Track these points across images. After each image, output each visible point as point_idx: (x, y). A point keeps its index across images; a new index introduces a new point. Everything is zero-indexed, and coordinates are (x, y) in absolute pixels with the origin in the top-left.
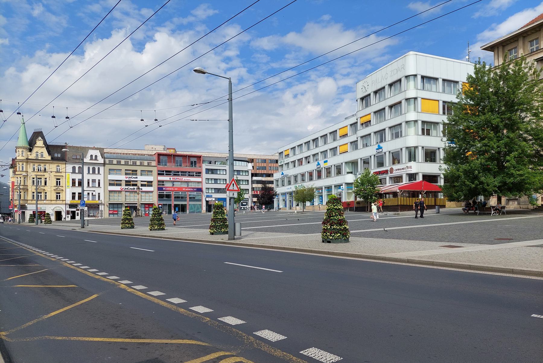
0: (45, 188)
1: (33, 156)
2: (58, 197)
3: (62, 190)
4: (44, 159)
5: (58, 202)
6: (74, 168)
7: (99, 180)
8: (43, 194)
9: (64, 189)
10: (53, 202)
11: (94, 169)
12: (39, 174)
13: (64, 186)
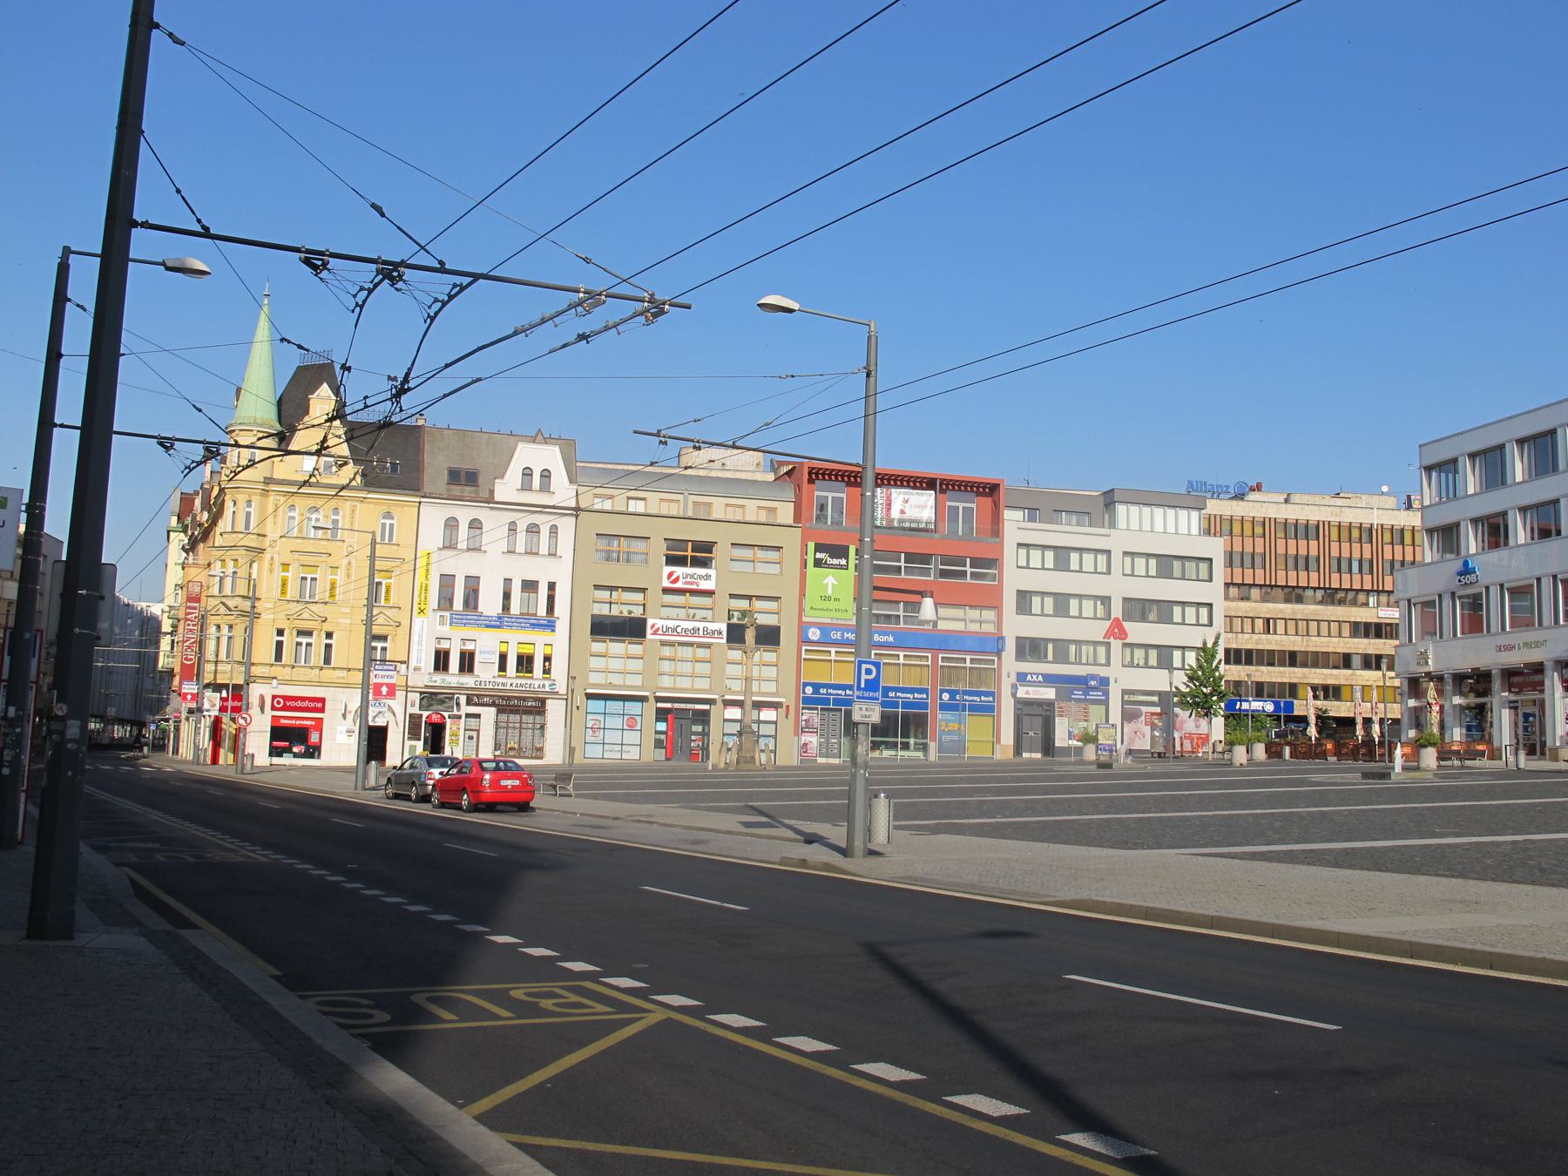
6: (451, 524)
7: (552, 586)
11: (533, 529)
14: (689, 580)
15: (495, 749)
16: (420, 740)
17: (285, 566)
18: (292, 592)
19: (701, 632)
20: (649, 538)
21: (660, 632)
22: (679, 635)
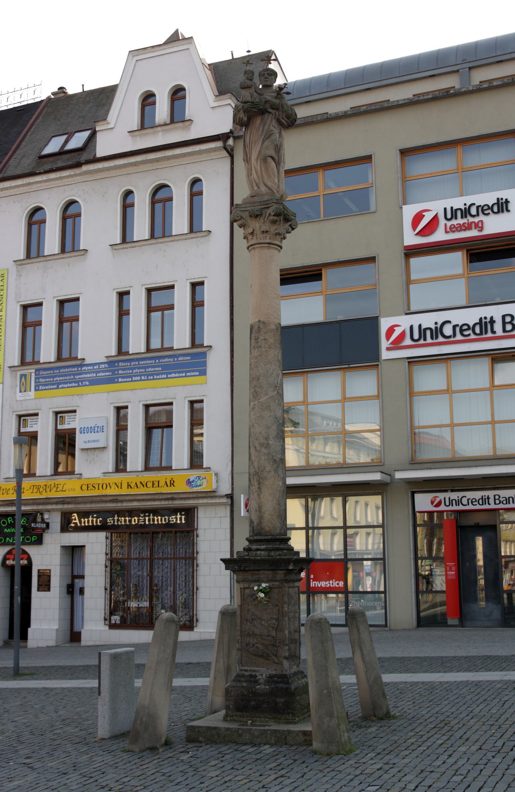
14: (460, 221)
15: (111, 614)
19: (498, 327)
20: (368, 159)
21: (408, 341)
22: (449, 340)
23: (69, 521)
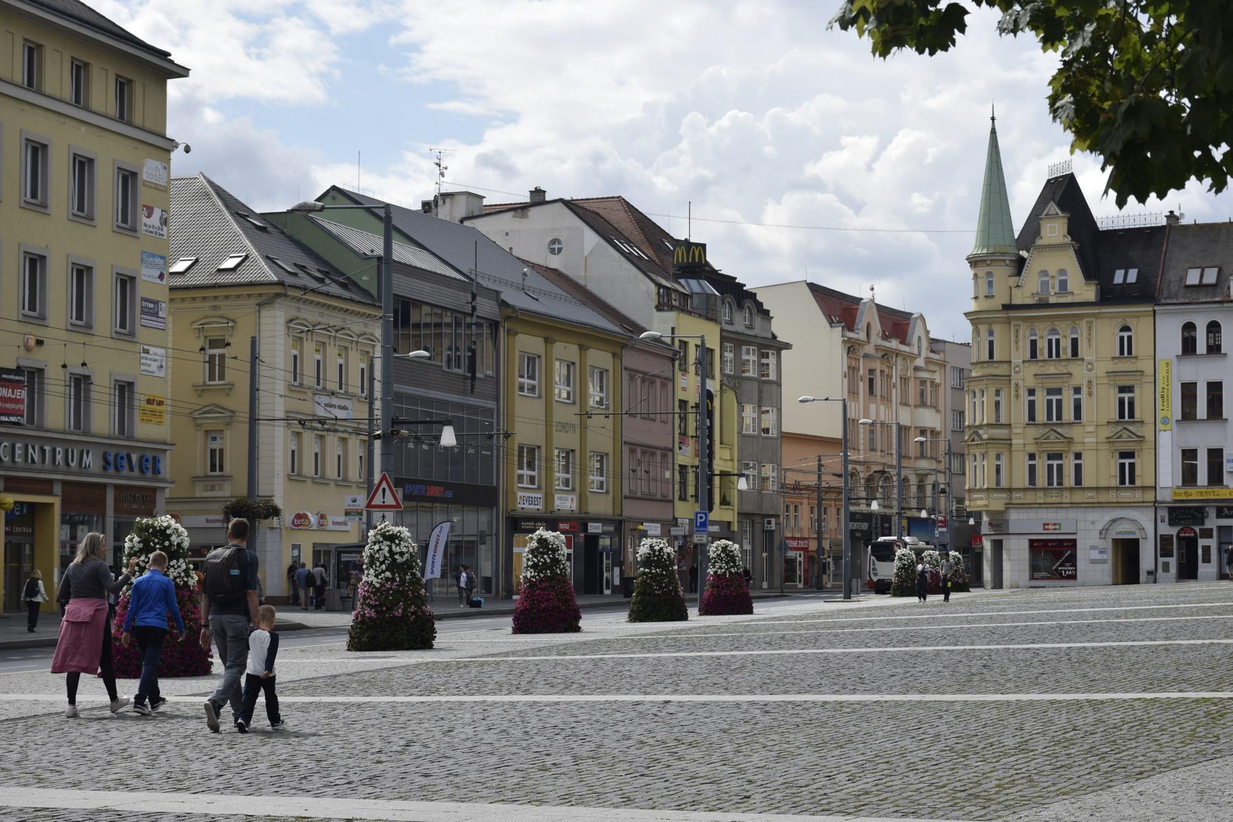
0: (1075, 433)
1: (1028, 289)
2: (1127, 476)
3: (1141, 439)
4: (1069, 299)
5: (1126, 496)
8: (1069, 464)
9: (1147, 432)
10: (1112, 497)
12: (1052, 369)
13: (1149, 418)
16: (1172, 556)
17: (1031, 392)
18: (1041, 416)
23: (1222, 512)
